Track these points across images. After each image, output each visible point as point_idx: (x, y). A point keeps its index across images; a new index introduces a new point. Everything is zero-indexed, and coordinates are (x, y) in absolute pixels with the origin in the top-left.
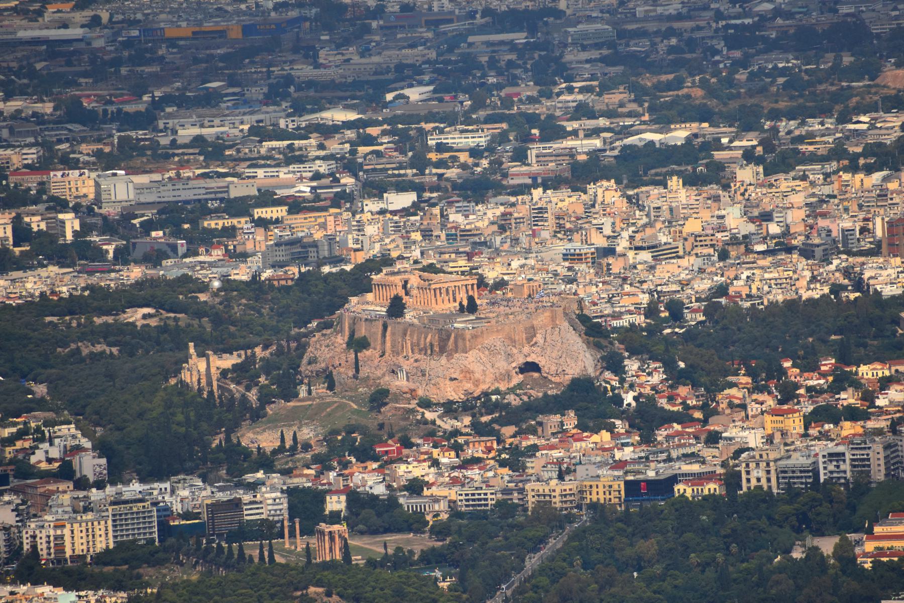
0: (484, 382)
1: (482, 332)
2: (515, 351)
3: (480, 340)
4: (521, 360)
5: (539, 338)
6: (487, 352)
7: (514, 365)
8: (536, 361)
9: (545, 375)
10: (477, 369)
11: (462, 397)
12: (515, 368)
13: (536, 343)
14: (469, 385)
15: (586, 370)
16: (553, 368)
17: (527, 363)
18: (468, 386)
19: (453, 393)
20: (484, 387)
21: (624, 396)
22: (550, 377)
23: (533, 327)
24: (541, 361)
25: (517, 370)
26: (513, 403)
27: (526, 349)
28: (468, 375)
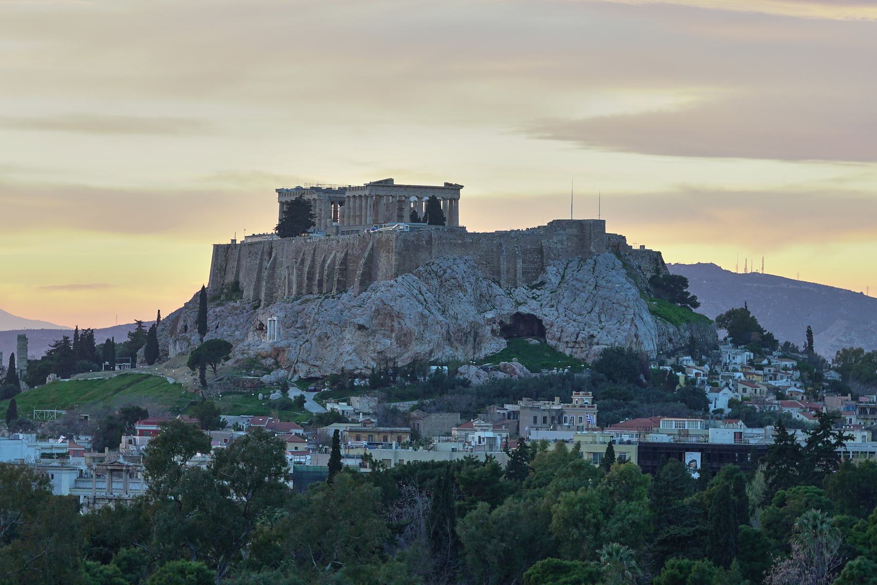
0: (421, 339)
1: (430, 242)
2: (497, 290)
3: (423, 255)
4: (508, 308)
5: (552, 274)
6: (435, 282)
7: (489, 315)
8: (538, 314)
9: (552, 342)
10: (410, 312)
11: (374, 364)
12: (493, 321)
13: (543, 283)
14: (388, 342)
15: (640, 344)
16: (571, 329)
17: (518, 317)
18: (387, 343)
19: (354, 357)
20: (418, 348)
21: (711, 396)
22: (561, 348)
23: (541, 252)
24: (547, 315)
25: (496, 327)
26: (475, 381)
27: (521, 292)
28: (388, 322)
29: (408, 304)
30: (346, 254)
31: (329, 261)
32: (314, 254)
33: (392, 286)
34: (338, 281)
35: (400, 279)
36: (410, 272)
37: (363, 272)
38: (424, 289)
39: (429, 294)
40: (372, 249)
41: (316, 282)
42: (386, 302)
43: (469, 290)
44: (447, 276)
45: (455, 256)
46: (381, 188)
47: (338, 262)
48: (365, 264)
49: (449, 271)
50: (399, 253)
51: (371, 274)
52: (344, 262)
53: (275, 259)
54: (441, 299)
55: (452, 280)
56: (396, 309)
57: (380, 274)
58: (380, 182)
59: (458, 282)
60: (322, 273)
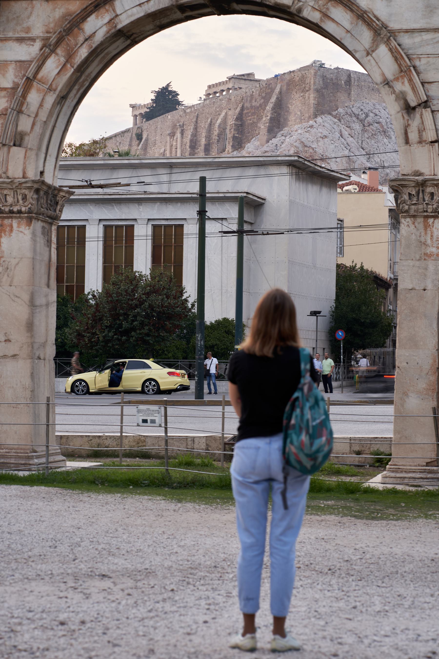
6: (357, 127)
29: (333, 146)
30: (242, 109)
31: (219, 121)
32: (196, 122)
33: (312, 127)
34: (234, 138)
35: (319, 119)
36: (330, 114)
37: (271, 117)
38: (346, 133)
39: (351, 139)
40: (280, 93)
41: (202, 147)
42: (307, 143)
43: (393, 138)
44: (369, 119)
45: (374, 102)
46: (243, 82)
47: (231, 122)
48: (273, 109)
49: (371, 115)
50: (317, 91)
51: (279, 121)
52: (240, 117)
53: (147, 140)
54: (365, 146)
55: (376, 125)
56: (320, 151)
57: (292, 118)
58: (243, 75)
59: (382, 127)
60: (208, 137)
